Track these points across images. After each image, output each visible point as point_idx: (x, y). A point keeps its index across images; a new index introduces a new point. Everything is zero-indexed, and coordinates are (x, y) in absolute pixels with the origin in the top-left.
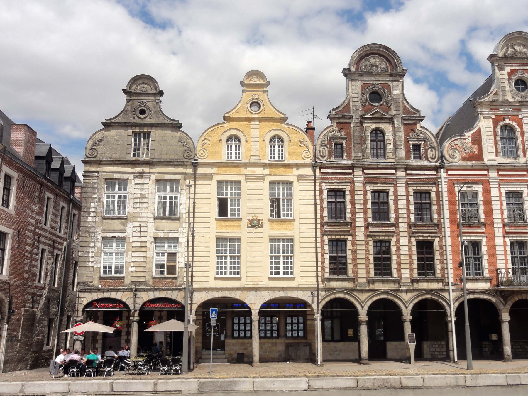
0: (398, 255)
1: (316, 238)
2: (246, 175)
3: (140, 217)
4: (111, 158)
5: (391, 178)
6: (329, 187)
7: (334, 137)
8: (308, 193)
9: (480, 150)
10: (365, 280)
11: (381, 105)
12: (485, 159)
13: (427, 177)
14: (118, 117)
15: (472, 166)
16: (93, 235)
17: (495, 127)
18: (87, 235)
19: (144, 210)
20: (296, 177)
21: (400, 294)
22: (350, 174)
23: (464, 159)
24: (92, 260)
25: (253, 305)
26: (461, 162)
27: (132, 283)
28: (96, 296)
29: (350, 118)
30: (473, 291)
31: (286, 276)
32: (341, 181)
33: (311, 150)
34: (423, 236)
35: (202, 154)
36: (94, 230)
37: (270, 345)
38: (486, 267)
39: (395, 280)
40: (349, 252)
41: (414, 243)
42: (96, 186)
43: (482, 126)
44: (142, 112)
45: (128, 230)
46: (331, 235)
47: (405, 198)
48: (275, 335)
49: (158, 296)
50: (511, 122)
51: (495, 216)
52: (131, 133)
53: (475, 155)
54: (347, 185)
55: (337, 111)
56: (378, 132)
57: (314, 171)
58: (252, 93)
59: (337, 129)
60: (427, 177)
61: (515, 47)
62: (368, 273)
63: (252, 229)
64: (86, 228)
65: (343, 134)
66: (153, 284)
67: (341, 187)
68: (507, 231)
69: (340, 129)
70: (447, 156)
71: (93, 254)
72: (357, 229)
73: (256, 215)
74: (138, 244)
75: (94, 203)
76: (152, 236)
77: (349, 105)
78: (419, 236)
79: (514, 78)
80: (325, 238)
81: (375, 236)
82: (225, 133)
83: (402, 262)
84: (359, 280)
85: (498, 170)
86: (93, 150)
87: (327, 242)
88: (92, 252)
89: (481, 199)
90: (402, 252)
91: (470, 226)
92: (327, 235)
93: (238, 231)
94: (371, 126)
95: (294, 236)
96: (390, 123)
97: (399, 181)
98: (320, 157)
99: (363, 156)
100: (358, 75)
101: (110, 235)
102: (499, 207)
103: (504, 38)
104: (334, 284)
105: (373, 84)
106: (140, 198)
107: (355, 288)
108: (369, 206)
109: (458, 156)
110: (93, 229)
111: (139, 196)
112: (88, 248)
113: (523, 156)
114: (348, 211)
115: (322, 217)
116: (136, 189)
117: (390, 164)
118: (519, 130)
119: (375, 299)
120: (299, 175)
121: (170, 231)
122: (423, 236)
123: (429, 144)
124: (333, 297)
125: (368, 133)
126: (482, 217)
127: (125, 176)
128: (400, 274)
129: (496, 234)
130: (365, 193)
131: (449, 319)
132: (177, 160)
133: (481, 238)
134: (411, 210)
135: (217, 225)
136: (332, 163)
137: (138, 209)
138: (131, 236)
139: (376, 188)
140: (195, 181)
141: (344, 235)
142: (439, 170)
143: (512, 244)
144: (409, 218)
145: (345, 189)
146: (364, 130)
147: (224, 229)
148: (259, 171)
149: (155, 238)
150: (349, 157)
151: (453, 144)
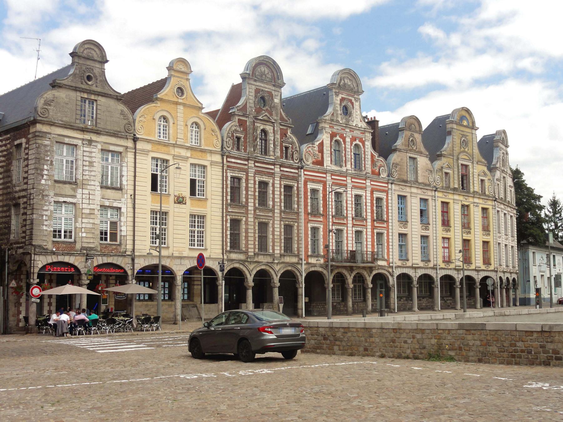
0: (273, 235)
1: (223, 217)
3: (89, 185)
4: (62, 121)
6: (232, 174)
9: (322, 157)
10: (252, 254)
12: (325, 165)
14: (68, 80)
16: (46, 198)
17: (331, 141)
18: (40, 197)
19: (92, 178)
20: (209, 162)
21: (273, 265)
22: (245, 165)
23: (313, 163)
25: (178, 272)
26: (311, 165)
27: (83, 248)
28: (51, 259)
29: (247, 117)
31: (199, 247)
32: (241, 170)
33: (220, 140)
34: (288, 221)
35: (139, 130)
37: (167, 307)
42: (49, 148)
44: (89, 78)
45: (79, 196)
48: (167, 298)
49: (106, 262)
50: (340, 139)
52: (79, 99)
58: (179, 79)
59: (238, 124)
62: (255, 248)
63: (178, 205)
64: (40, 190)
66: (101, 250)
67: (240, 175)
68: (334, 221)
70: (304, 159)
71: (47, 217)
73: (182, 192)
74: (87, 211)
75: (47, 166)
78: (286, 221)
79: (343, 104)
80: (228, 217)
82: (158, 114)
84: (250, 254)
87: (229, 221)
88: (46, 215)
91: (315, 216)
92: (229, 215)
93: (167, 206)
94: (260, 126)
98: (226, 147)
99: (254, 150)
101: (62, 199)
104: (234, 256)
105: (262, 90)
107: (246, 260)
108: (257, 194)
109: (310, 160)
110: (46, 193)
111: (87, 163)
112: (42, 211)
115: (227, 200)
116: (85, 156)
117: (272, 160)
118: (343, 146)
119: (258, 269)
120: (212, 161)
122: (288, 221)
126: (322, 209)
127: (75, 142)
128: (274, 250)
131: (301, 286)
132: (120, 132)
133: (320, 226)
137: (87, 176)
141: (241, 216)
142: (300, 170)
144: (280, 206)
149: (101, 206)
150: (245, 150)
151: (308, 150)
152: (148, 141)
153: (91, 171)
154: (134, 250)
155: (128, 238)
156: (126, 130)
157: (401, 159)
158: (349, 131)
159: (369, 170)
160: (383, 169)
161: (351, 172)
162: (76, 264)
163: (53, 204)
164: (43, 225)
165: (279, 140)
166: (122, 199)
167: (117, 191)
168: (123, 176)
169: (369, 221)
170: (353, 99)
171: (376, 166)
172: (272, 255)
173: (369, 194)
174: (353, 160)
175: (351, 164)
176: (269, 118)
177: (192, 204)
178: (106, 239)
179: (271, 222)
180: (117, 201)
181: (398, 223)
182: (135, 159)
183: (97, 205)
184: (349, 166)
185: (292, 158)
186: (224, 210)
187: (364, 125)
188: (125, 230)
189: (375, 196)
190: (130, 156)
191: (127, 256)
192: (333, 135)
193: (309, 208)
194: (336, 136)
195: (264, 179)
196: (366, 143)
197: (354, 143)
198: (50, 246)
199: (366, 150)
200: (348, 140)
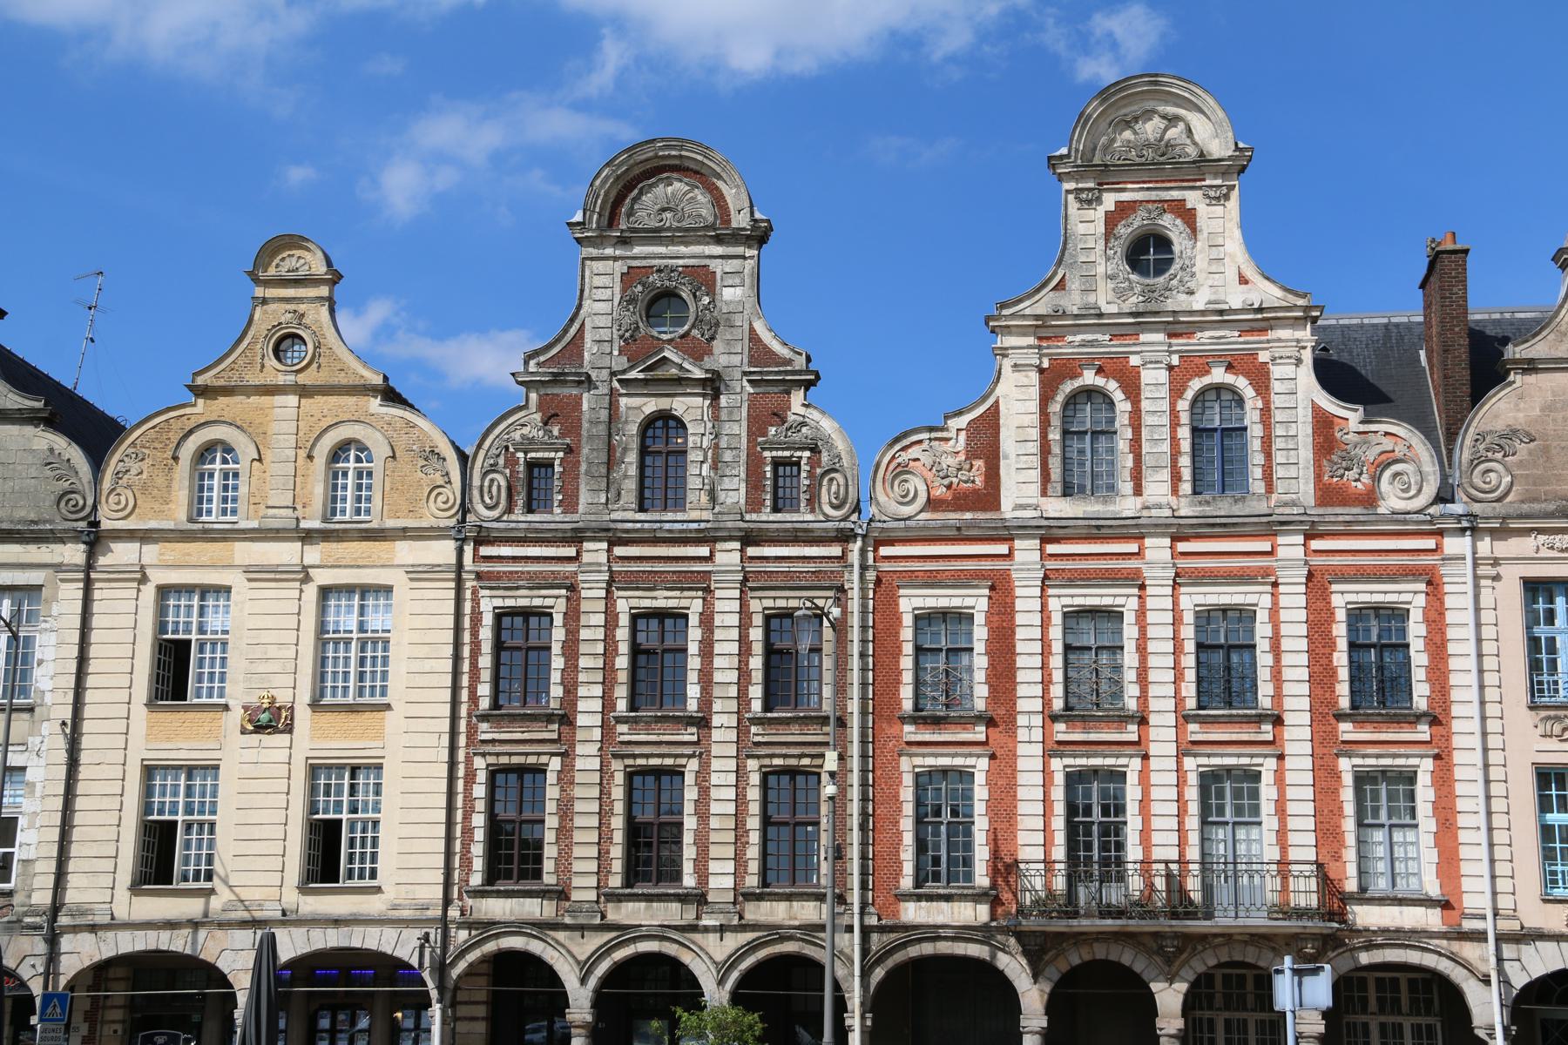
0: (703, 815)
2: (248, 570)
5: (698, 572)
6: (499, 602)
7: (528, 444)
8: (434, 622)
10: (592, 896)
11: (682, 337)
13: (811, 567)
15: (959, 529)
17: (1045, 400)
21: (697, 937)
22: (569, 559)
30: (932, 933)
34: (785, 756)
38: (981, 854)
39: (687, 895)
40: (551, 807)
41: (755, 779)
43: (1006, 396)
47: (735, 634)
51: (1021, 690)
53: (976, 491)
54: (557, 597)
55: (542, 359)
56: (672, 423)
57: (460, 552)
59: (538, 417)
60: (811, 567)
61: (1137, 127)
62: (602, 871)
65: (556, 432)
67: (537, 602)
69: (549, 418)
72: (580, 735)
73: (273, 692)
77: (582, 338)
79: (1124, 231)
80: (479, 763)
81: (634, 756)
82: (192, 438)
83: (713, 837)
84: (575, 896)
85: (1045, 540)
89: (980, 633)
90: (715, 808)
91: (937, 722)
92: (484, 755)
95: (384, 757)
96: (704, 396)
100: (615, 240)
102: (1037, 661)
103: (1095, 98)
104: (496, 908)
113: (1131, 492)
114: (556, 677)
117: (695, 526)
119: (619, 955)
122: (785, 756)
123: (825, 457)
124: (491, 947)
125: (633, 429)
126: (982, 690)
128: (702, 874)
129: (1022, 749)
130: (611, 623)
132: (36, 523)
133: (970, 761)
134: (753, 673)
135: (150, 727)
136: (513, 525)
139: (647, 603)
141: (539, 754)
143: (1074, 779)
144: (743, 698)
145: (552, 607)
146: (623, 419)
147: (169, 739)
148: (286, 553)
150: (570, 504)
151: (904, 456)
152: (144, 537)
154: (56, 908)
155: (39, 867)
156: (121, 514)
157: (1548, 408)
159: (1306, 491)
160: (1396, 475)
161: (1168, 513)
165: (744, 440)
166: (30, 739)
170: (1193, 199)
171: (1349, 462)
172: (699, 898)
173: (1294, 600)
174: (1185, 461)
175: (1176, 478)
177: (313, 729)
179: (693, 765)
181: (1530, 718)
184: (1157, 488)
185: (813, 502)
186: (462, 740)
189: (1337, 601)
190: (71, 594)
195: (661, 603)
196: (1276, 371)
197: (1196, 385)
199: (1277, 401)
200: (1154, 379)
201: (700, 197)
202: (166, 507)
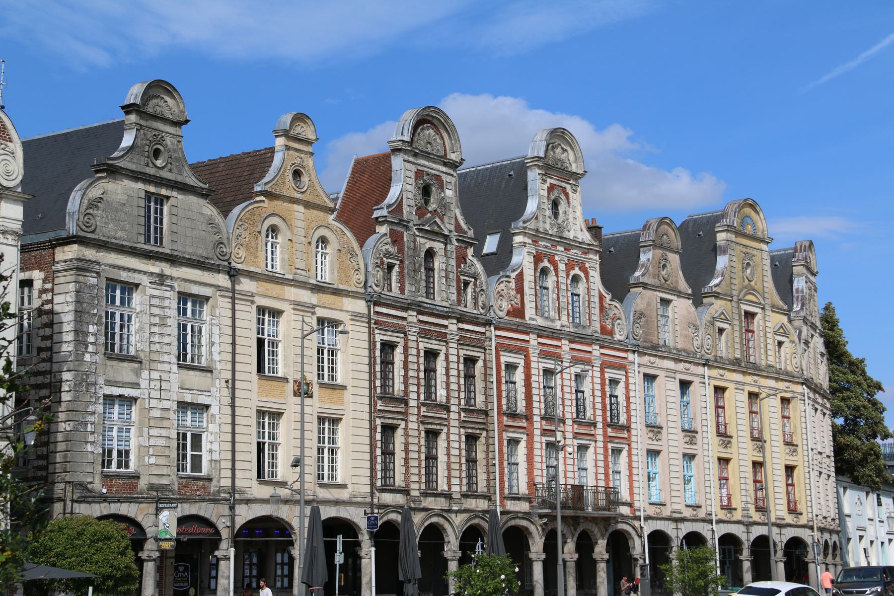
3: (160, 362)
4: (116, 238)
7: (388, 254)
12: (527, 318)
19: (166, 348)
24: (91, 438)
26: (506, 318)
27: (152, 487)
34: (472, 428)
36: (93, 380)
45: (144, 384)
46: (385, 418)
49: (188, 513)
54: (401, 338)
59: (389, 240)
67: (395, 339)
74: (156, 414)
76: (176, 399)
78: (469, 428)
81: (428, 423)
86: (90, 216)
87: (379, 429)
92: (380, 417)
97: (451, 339)
100: (413, 153)
101: (116, 391)
104: (388, 498)
106: (160, 325)
110: (92, 379)
116: (154, 306)
121: (200, 393)
128: (449, 485)
132: (207, 258)
137: (157, 344)
138: (146, 396)
140: (234, 304)
141: (398, 419)
147: (267, 396)
149: (179, 402)
153: (163, 335)
158: (562, 249)
162: (139, 519)
163: (101, 401)
164: (87, 442)
167: (204, 374)
168: (213, 344)
169: (600, 425)
176: (439, 227)
178: (184, 469)
180: (204, 393)
182: (234, 310)
183: (173, 401)
184: (564, 318)
187: (586, 237)
188: (218, 449)
191: (223, 502)
192: (537, 259)
193: (504, 401)
194: (542, 261)
198: (98, 486)
201: (438, 140)
202: (256, 260)
